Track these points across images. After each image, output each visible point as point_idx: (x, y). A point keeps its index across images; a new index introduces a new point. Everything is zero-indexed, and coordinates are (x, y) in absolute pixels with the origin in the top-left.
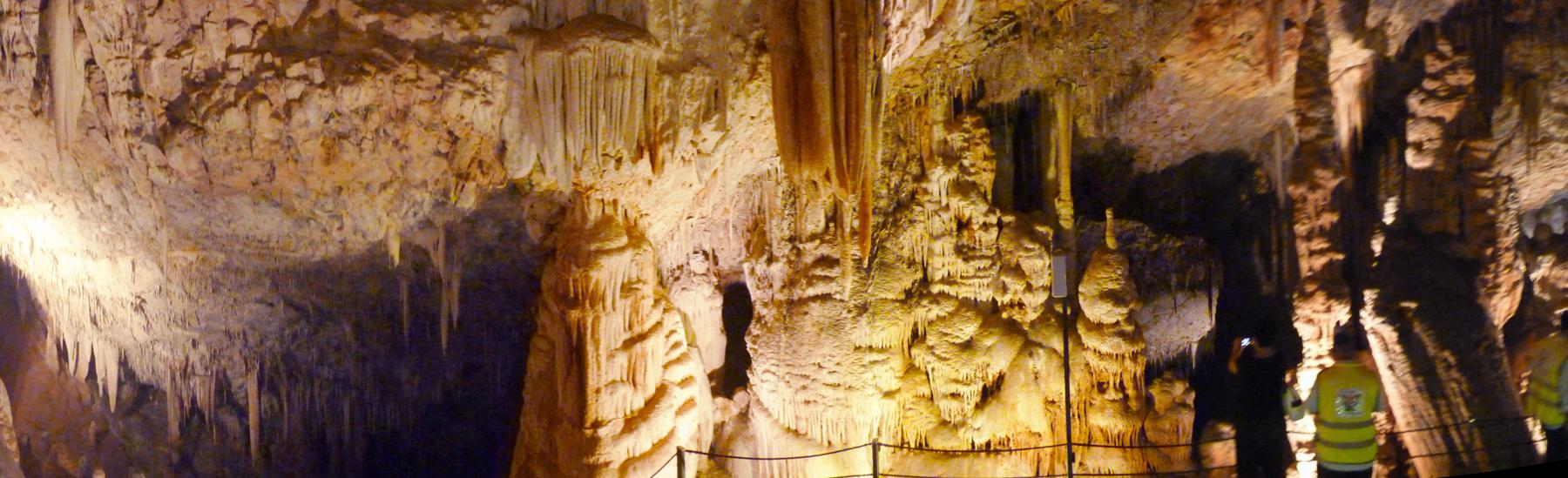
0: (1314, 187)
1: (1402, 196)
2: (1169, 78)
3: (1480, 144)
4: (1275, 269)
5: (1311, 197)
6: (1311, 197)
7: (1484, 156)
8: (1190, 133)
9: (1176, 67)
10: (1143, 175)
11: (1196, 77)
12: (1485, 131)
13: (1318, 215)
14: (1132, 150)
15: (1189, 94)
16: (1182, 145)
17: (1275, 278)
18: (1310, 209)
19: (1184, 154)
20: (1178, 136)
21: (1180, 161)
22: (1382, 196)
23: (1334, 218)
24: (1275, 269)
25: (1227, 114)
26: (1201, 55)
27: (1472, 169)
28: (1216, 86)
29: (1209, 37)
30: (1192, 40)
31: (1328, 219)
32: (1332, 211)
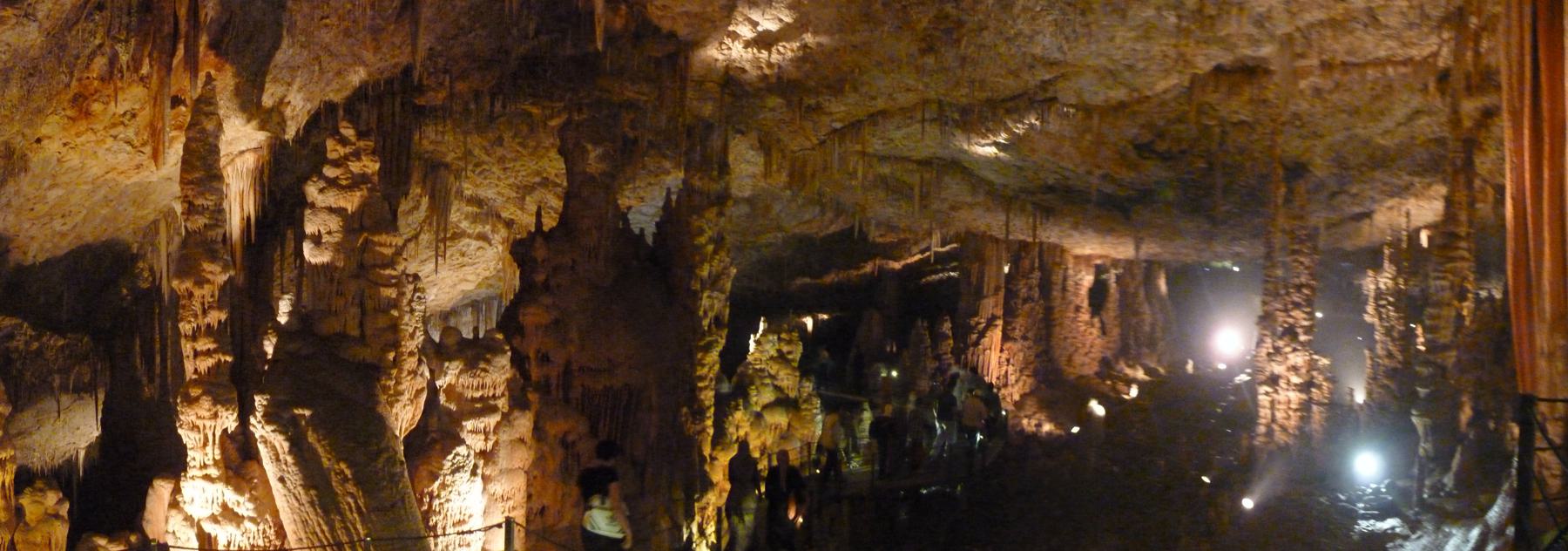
0: (200, 282)
1: (298, 296)
2: (46, 161)
3: (383, 238)
4: (158, 371)
5: (197, 292)
6: (197, 292)
7: (388, 251)
8: (70, 223)
9: (52, 147)
10: (20, 269)
11: (74, 159)
12: (391, 225)
13: (205, 312)
14: (9, 240)
15: (65, 179)
16: (63, 235)
17: (157, 381)
18: (197, 307)
19: (65, 246)
20: (57, 225)
21: (60, 253)
22: (276, 293)
23: (223, 316)
24: (158, 371)
25: (107, 200)
26: (78, 135)
27: (375, 266)
28: (95, 169)
29: (88, 114)
30: (70, 118)
31: (216, 317)
32: (220, 308)
